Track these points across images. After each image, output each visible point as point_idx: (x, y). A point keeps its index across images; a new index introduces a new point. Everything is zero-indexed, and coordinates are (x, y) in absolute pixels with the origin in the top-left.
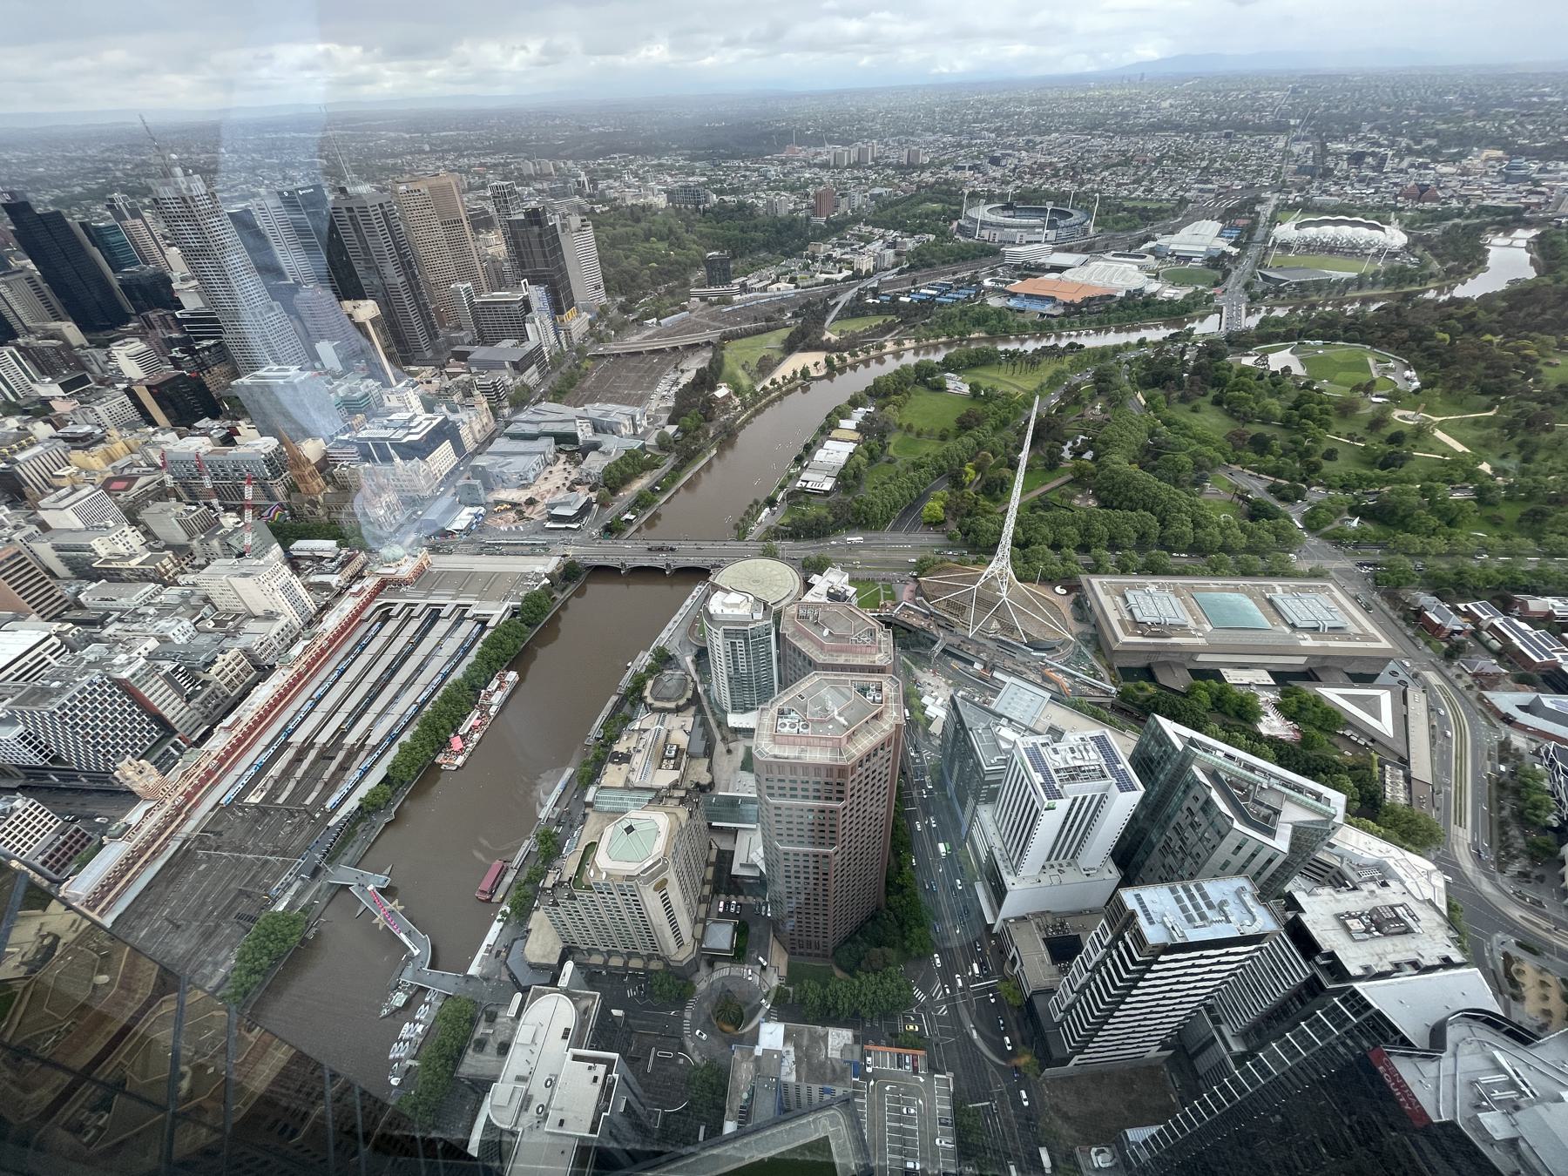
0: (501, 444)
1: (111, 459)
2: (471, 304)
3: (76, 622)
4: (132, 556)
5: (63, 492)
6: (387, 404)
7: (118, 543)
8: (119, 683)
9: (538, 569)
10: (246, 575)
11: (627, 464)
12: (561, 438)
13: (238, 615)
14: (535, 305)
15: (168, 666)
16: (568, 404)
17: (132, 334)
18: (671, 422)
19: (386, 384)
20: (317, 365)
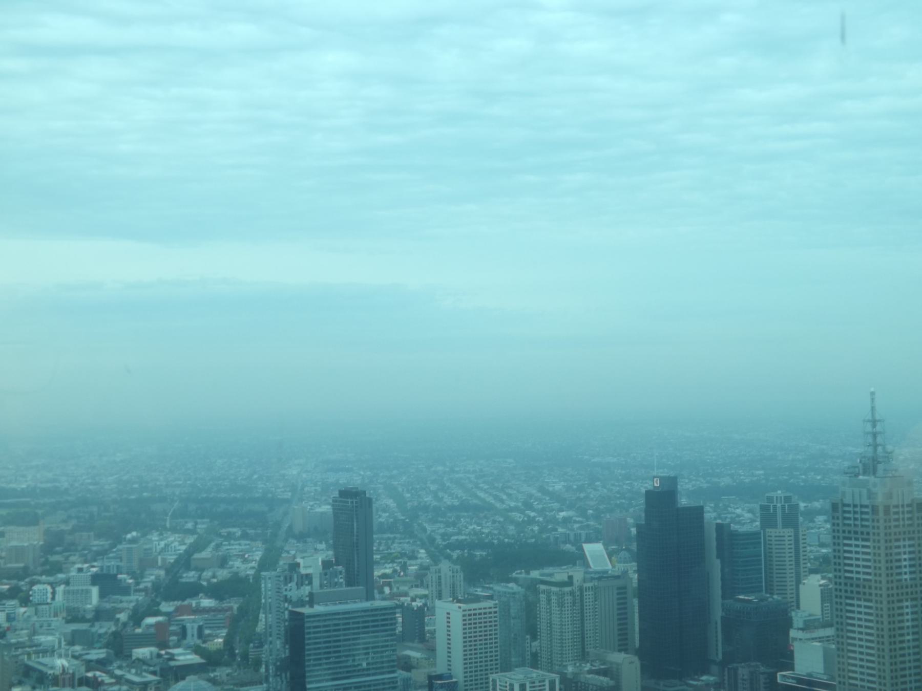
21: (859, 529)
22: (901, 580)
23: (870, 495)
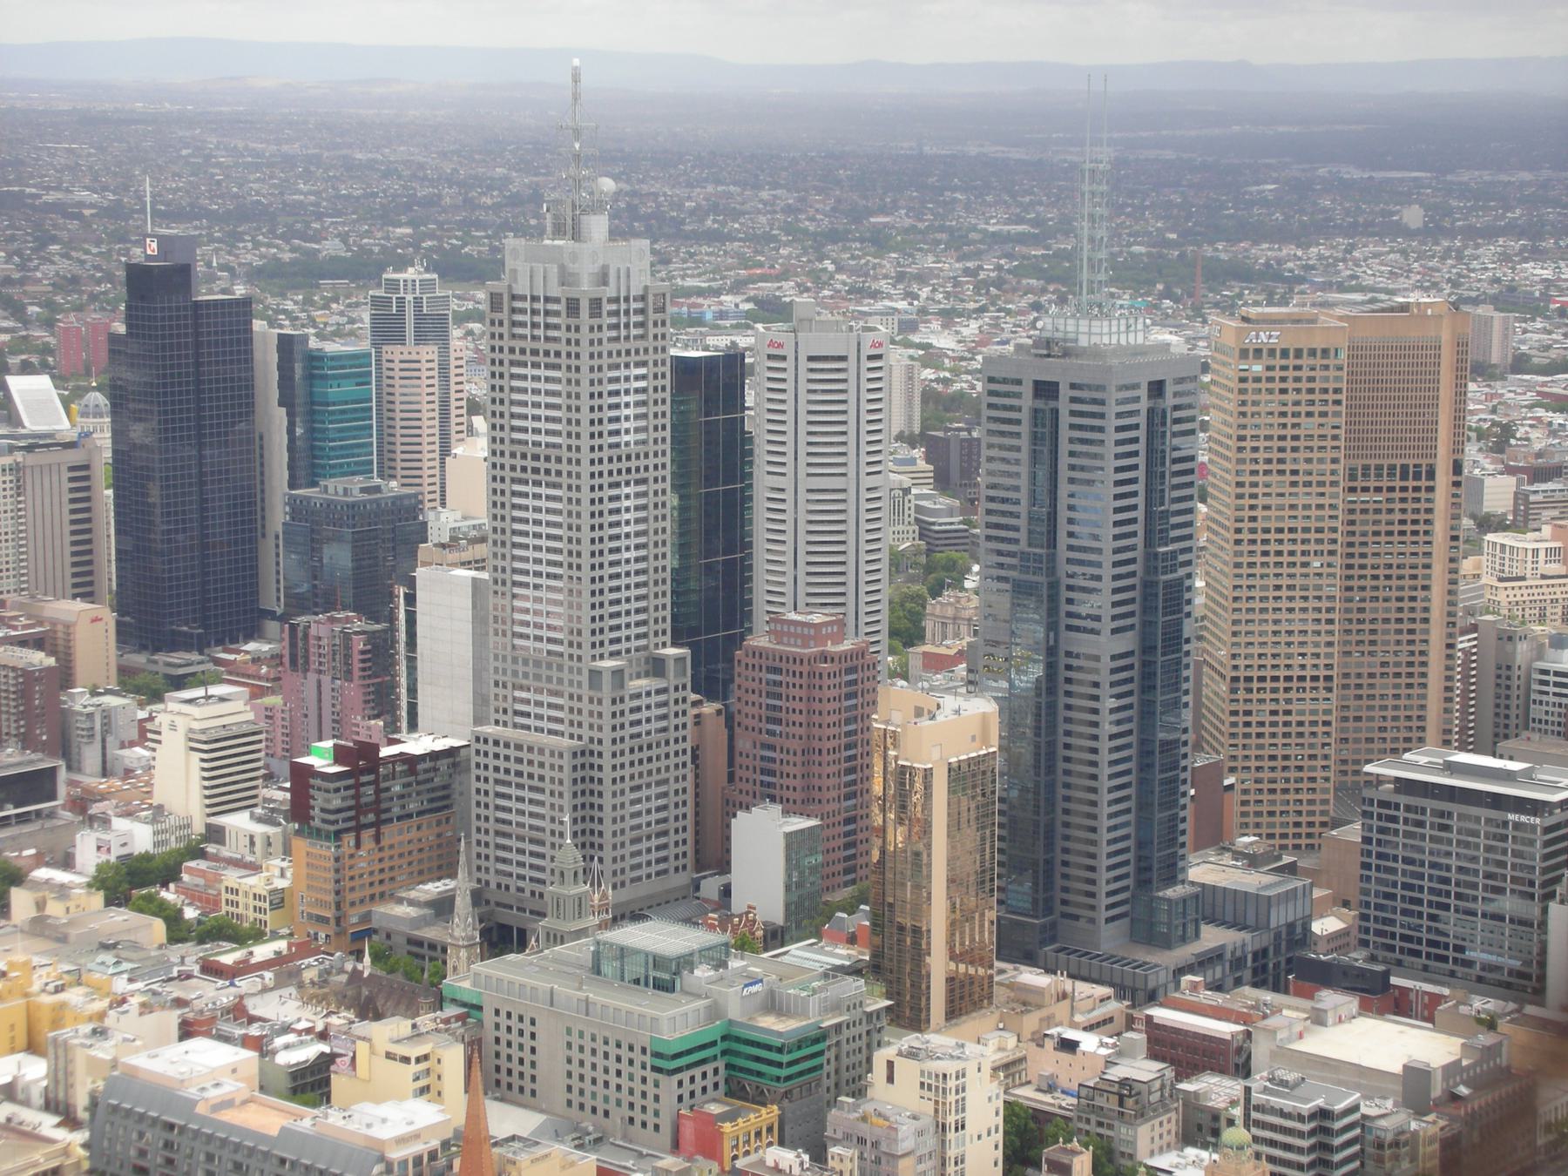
17: (234, 673)
19: (908, 1012)
21: (541, 346)
22: (618, 445)
23: (566, 278)
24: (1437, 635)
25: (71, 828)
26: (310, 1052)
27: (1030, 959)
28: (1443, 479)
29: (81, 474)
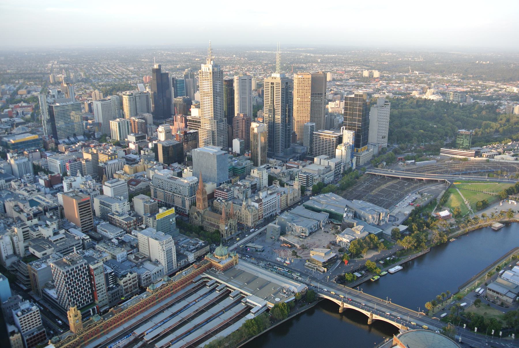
0: (299, 210)
1: (136, 171)
2: (312, 134)
3: (91, 237)
4: (122, 215)
5: (114, 180)
6: (252, 174)
7: (119, 207)
8: (89, 269)
9: (293, 289)
10: (156, 239)
11: (366, 242)
12: (333, 216)
13: (145, 257)
14: (345, 140)
15: (109, 270)
16: (345, 197)
18: (404, 224)
19: (256, 165)
20: (230, 149)
24: (323, 115)
25: (149, 143)
26: (180, 171)
27: (271, 157)
28: (324, 94)
29: (147, 96)
